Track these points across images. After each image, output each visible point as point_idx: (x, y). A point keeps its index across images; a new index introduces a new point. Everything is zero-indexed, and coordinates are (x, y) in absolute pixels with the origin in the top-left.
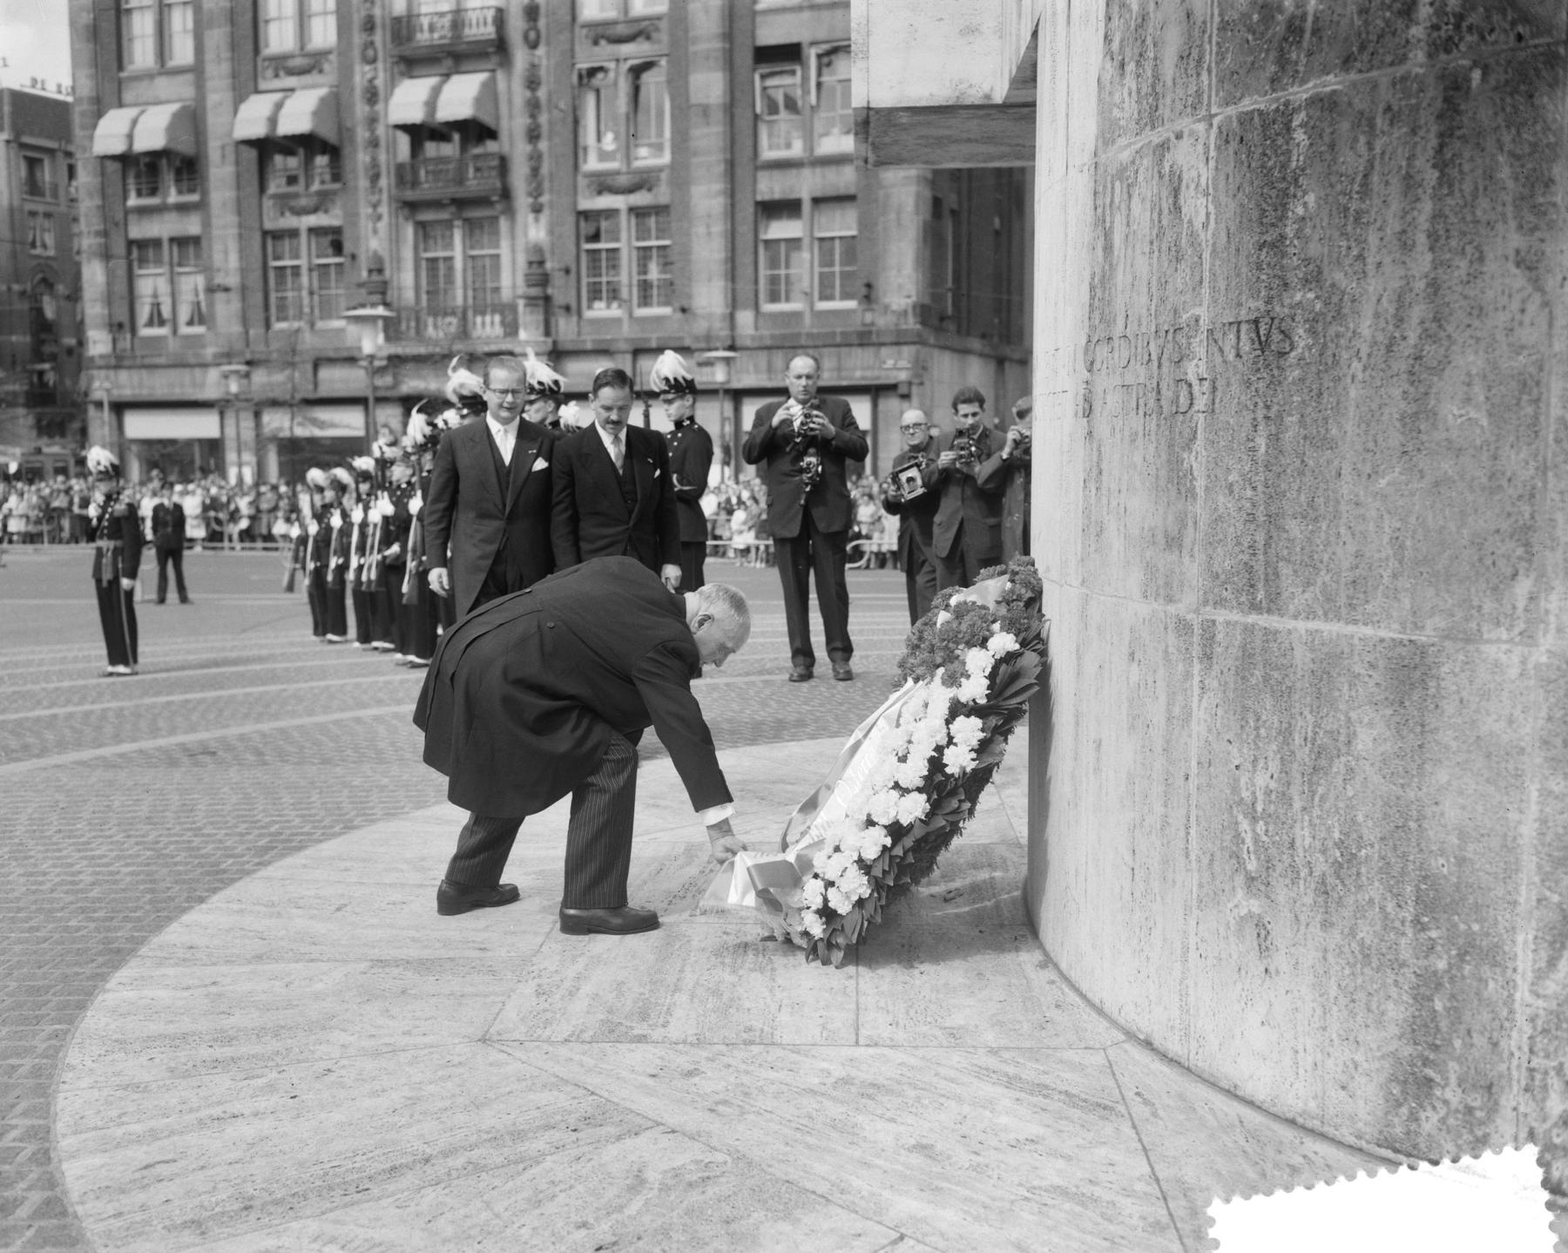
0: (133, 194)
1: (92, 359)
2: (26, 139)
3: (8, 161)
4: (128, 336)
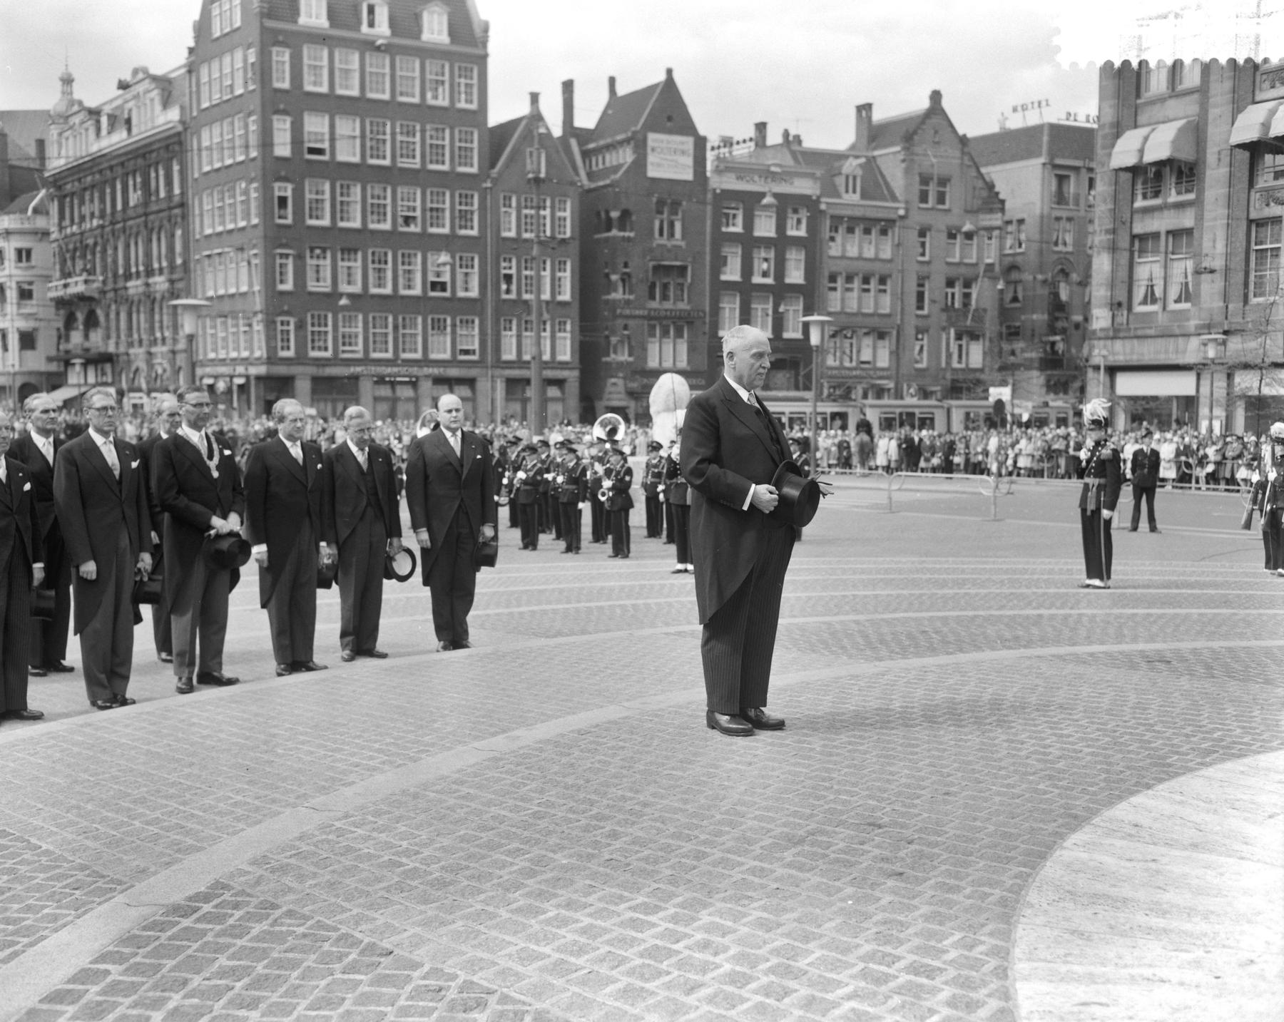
0: (1140, 197)
1: (1094, 332)
2: (1059, 161)
3: (1043, 179)
4: (1125, 313)
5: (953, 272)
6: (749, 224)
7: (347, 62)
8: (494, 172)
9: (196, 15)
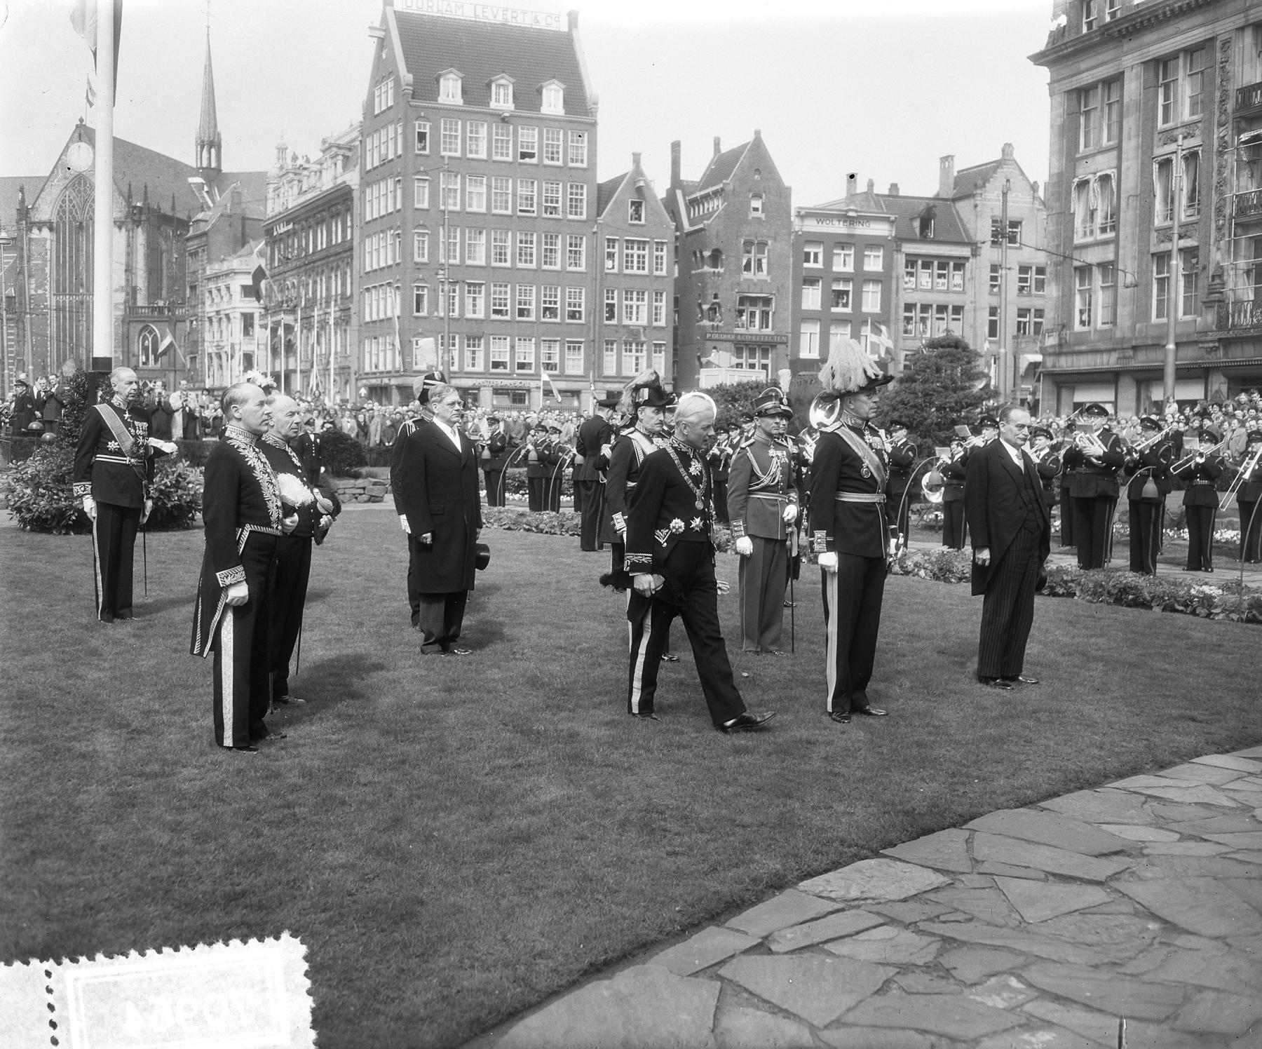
5: (1025, 302)
6: (828, 262)
7: (477, 132)
8: (600, 220)
9: (364, 96)
